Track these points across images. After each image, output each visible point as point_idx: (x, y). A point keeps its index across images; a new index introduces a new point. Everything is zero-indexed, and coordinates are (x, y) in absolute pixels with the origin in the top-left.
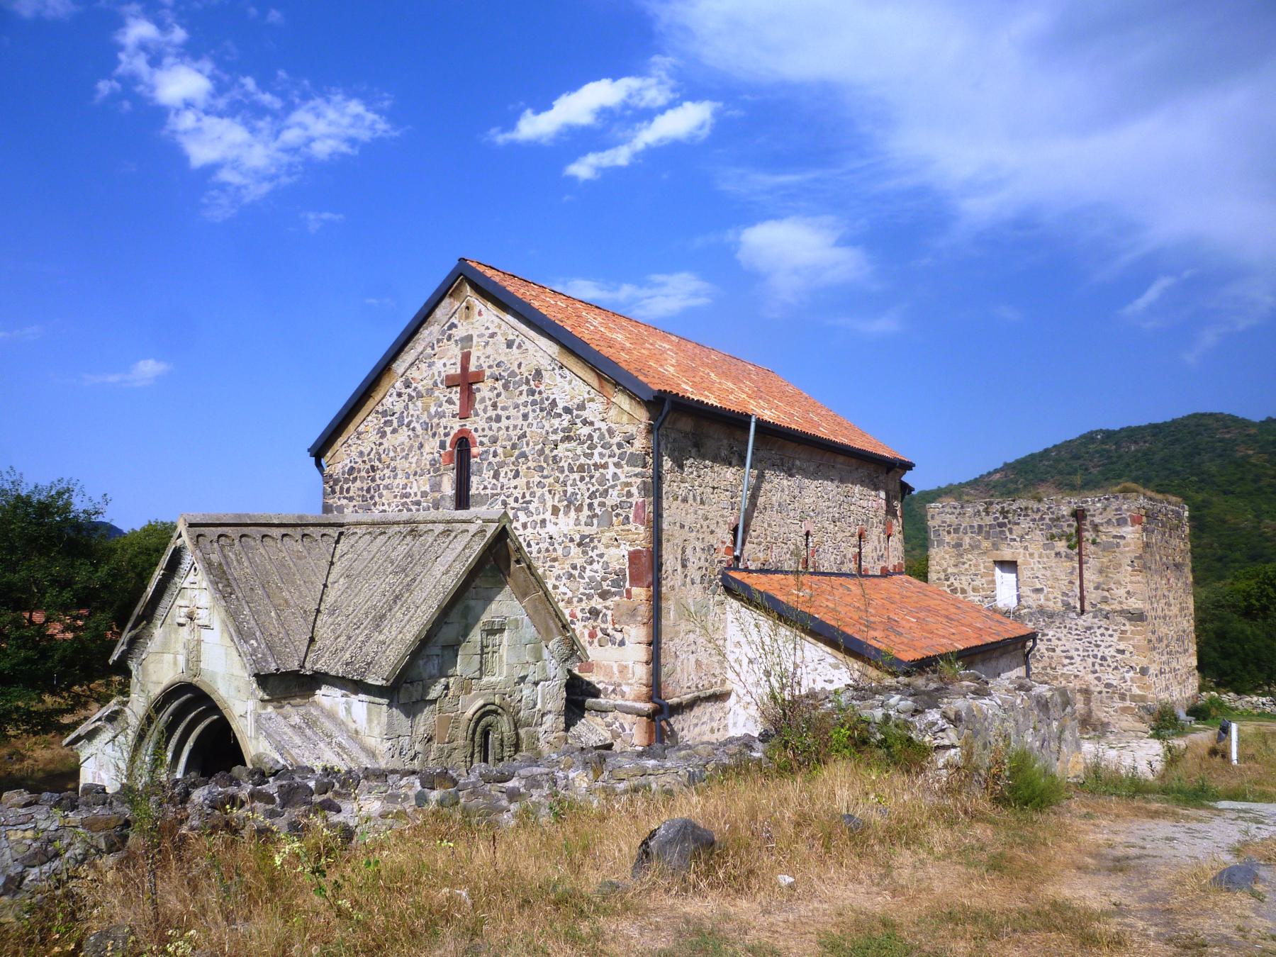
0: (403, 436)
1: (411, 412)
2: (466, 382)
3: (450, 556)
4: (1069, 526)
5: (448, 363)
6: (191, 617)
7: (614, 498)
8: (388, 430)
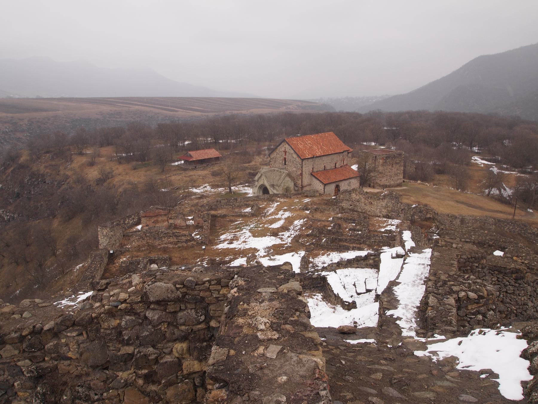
0: (279, 156)
2: (285, 152)
3: (284, 175)
4: (374, 158)
5: (283, 149)
6: (263, 179)
7: (299, 168)
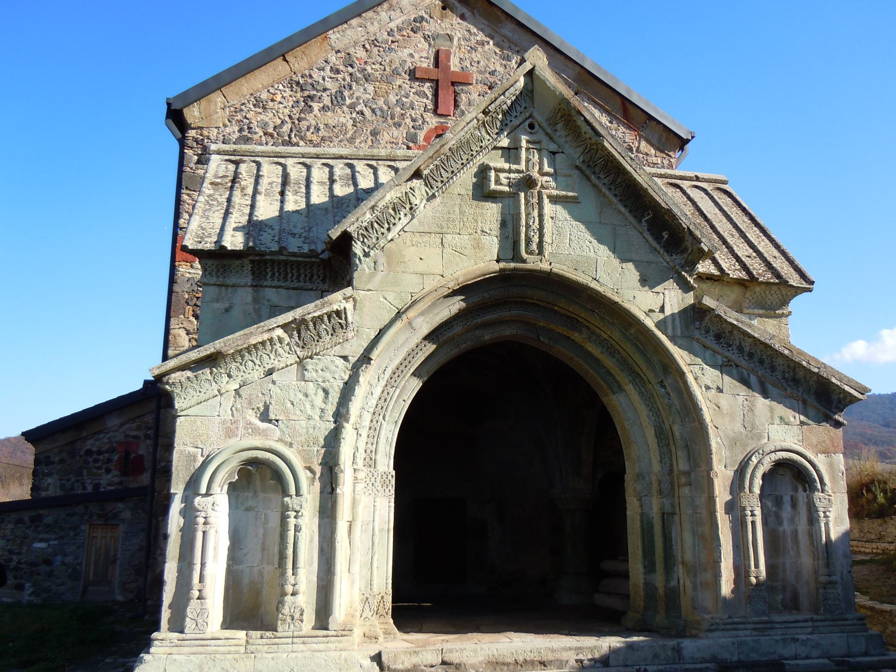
0: (344, 117)
1: (357, 94)
8: (316, 106)
